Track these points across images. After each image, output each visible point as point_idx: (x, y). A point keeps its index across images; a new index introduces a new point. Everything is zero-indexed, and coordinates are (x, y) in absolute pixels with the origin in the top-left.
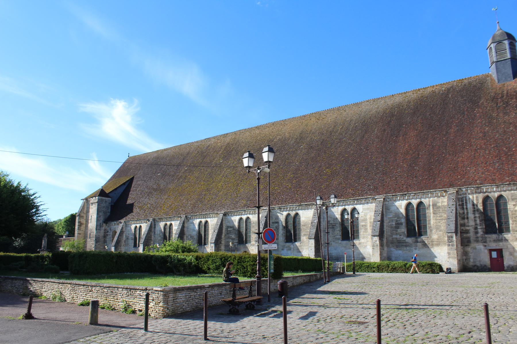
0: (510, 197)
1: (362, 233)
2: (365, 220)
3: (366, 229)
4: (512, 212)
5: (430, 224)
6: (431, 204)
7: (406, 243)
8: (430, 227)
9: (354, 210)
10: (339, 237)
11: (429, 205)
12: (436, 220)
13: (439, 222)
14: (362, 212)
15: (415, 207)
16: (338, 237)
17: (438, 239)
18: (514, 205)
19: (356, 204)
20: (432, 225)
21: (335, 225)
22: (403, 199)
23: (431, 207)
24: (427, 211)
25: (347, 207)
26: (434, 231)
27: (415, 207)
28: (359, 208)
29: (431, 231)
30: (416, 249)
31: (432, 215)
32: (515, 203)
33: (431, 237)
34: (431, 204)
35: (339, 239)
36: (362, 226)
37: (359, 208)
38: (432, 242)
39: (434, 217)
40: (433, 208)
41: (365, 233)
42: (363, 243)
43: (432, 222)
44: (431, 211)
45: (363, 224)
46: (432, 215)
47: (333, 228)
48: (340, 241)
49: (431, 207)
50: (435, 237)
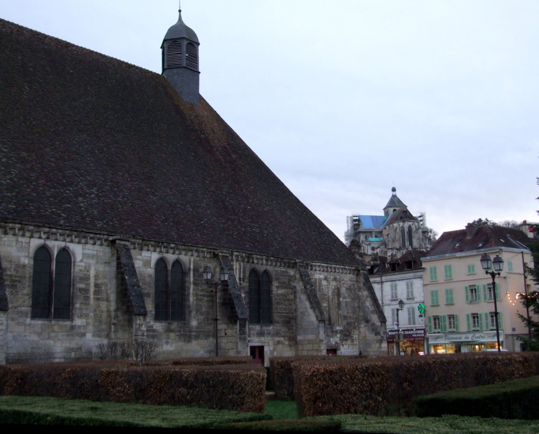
0: (274, 275)
1: (78, 305)
2: (86, 278)
3: (87, 298)
4: (275, 295)
5: (189, 301)
6: (192, 267)
7: (154, 331)
8: (189, 307)
9: (65, 252)
10: (29, 309)
11: (190, 269)
12: (197, 295)
13: (201, 300)
14: (81, 261)
15: (170, 268)
16: (23, 308)
17: (197, 328)
18: (277, 287)
19: (71, 241)
20: (191, 303)
21: (19, 282)
22: (155, 251)
23: (192, 273)
24: (187, 279)
25: (51, 243)
26: (193, 313)
27: (170, 268)
28: (77, 250)
29: (190, 312)
30: (167, 343)
31: (192, 287)
32: (277, 285)
33: (189, 324)
34: (192, 267)
35: (26, 315)
36: (80, 290)
37: (77, 250)
38: (191, 331)
39: (194, 290)
40: (194, 274)
41: (83, 307)
42: (80, 327)
43: (191, 299)
44: (192, 279)
45: (82, 286)
46: (192, 287)
47: (13, 286)
48: (28, 320)
49: (192, 273)
50: (194, 323)
